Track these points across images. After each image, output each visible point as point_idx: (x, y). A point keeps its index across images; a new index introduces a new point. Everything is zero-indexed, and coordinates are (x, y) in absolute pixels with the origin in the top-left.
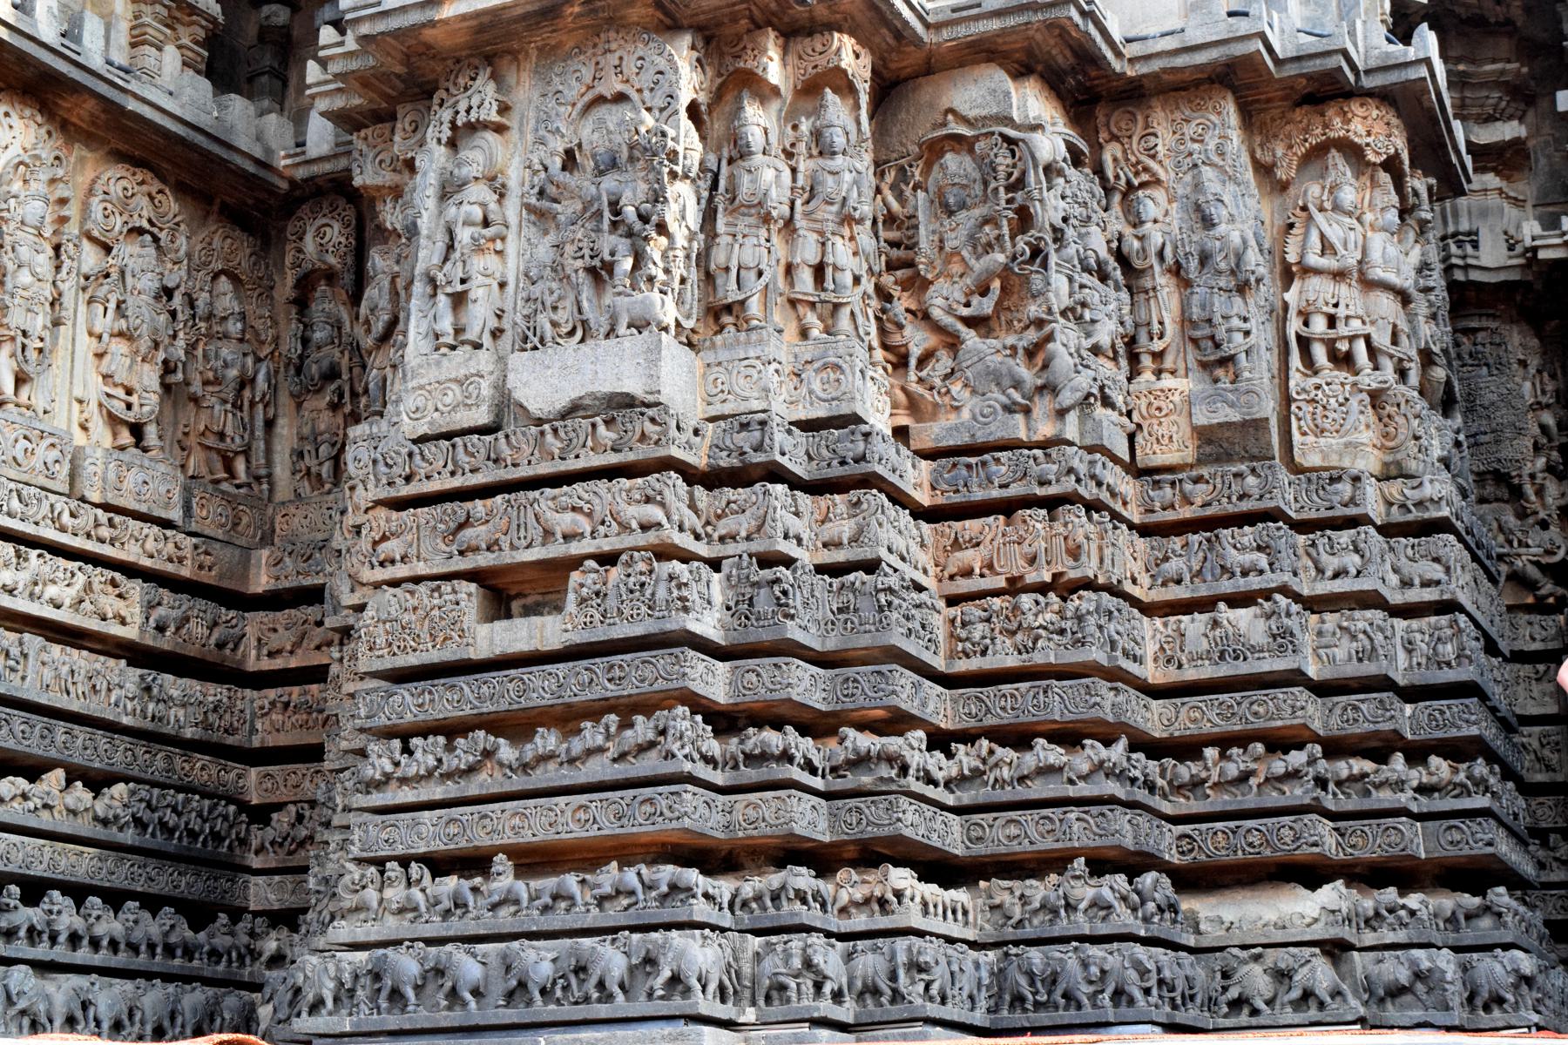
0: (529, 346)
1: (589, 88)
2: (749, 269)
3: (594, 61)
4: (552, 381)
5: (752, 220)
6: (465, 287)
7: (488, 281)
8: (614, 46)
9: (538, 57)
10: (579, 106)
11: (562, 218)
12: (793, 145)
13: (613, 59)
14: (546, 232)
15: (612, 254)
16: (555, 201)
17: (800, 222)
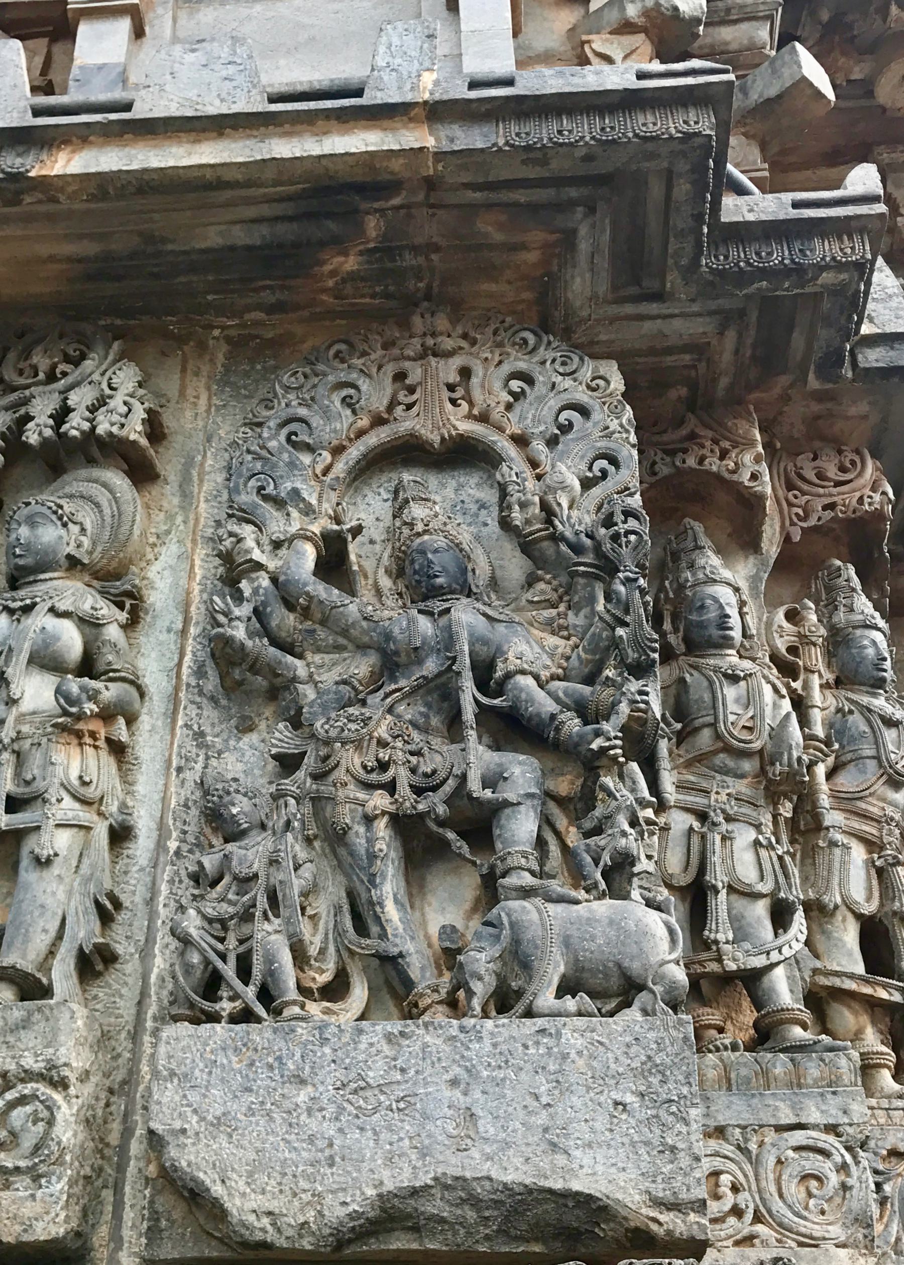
0: (226, 1006)
1: (379, 421)
2: (756, 896)
3: (390, 369)
4: (313, 1124)
5: (741, 787)
6: (20, 819)
7: (85, 816)
8: (448, 344)
9: (229, 357)
10: (354, 452)
11: (308, 692)
12: (793, 650)
13: (449, 371)
14: (246, 727)
15: (487, 783)
16: (289, 648)
17: (833, 818)
